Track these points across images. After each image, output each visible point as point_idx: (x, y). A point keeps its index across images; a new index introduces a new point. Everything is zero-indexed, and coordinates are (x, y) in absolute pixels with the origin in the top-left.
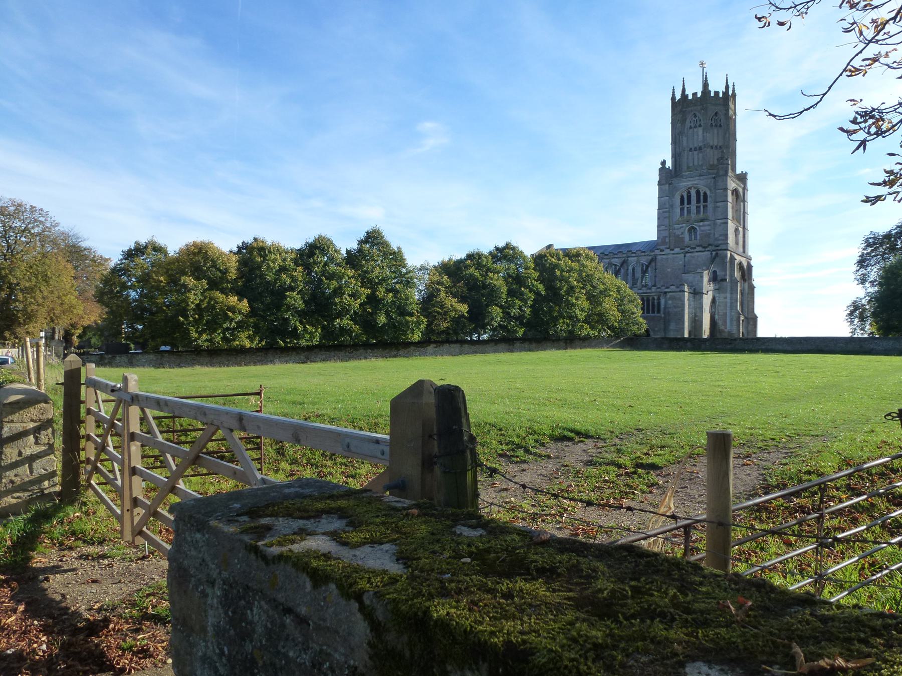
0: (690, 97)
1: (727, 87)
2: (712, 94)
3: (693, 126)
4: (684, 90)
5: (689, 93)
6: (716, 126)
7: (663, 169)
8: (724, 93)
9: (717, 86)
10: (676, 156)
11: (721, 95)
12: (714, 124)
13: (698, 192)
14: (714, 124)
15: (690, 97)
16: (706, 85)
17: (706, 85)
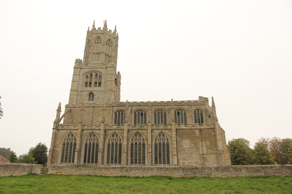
0: (97, 29)
1: (115, 30)
2: (108, 30)
3: (97, 42)
4: (94, 26)
5: (97, 27)
6: (109, 45)
7: (78, 61)
8: (113, 32)
9: (111, 27)
10: (86, 56)
11: (112, 33)
12: (108, 44)
13: (97, 75)
14: (108, 44)
15: (97, 29)
16: (105, 25)
17: (105, 25)
